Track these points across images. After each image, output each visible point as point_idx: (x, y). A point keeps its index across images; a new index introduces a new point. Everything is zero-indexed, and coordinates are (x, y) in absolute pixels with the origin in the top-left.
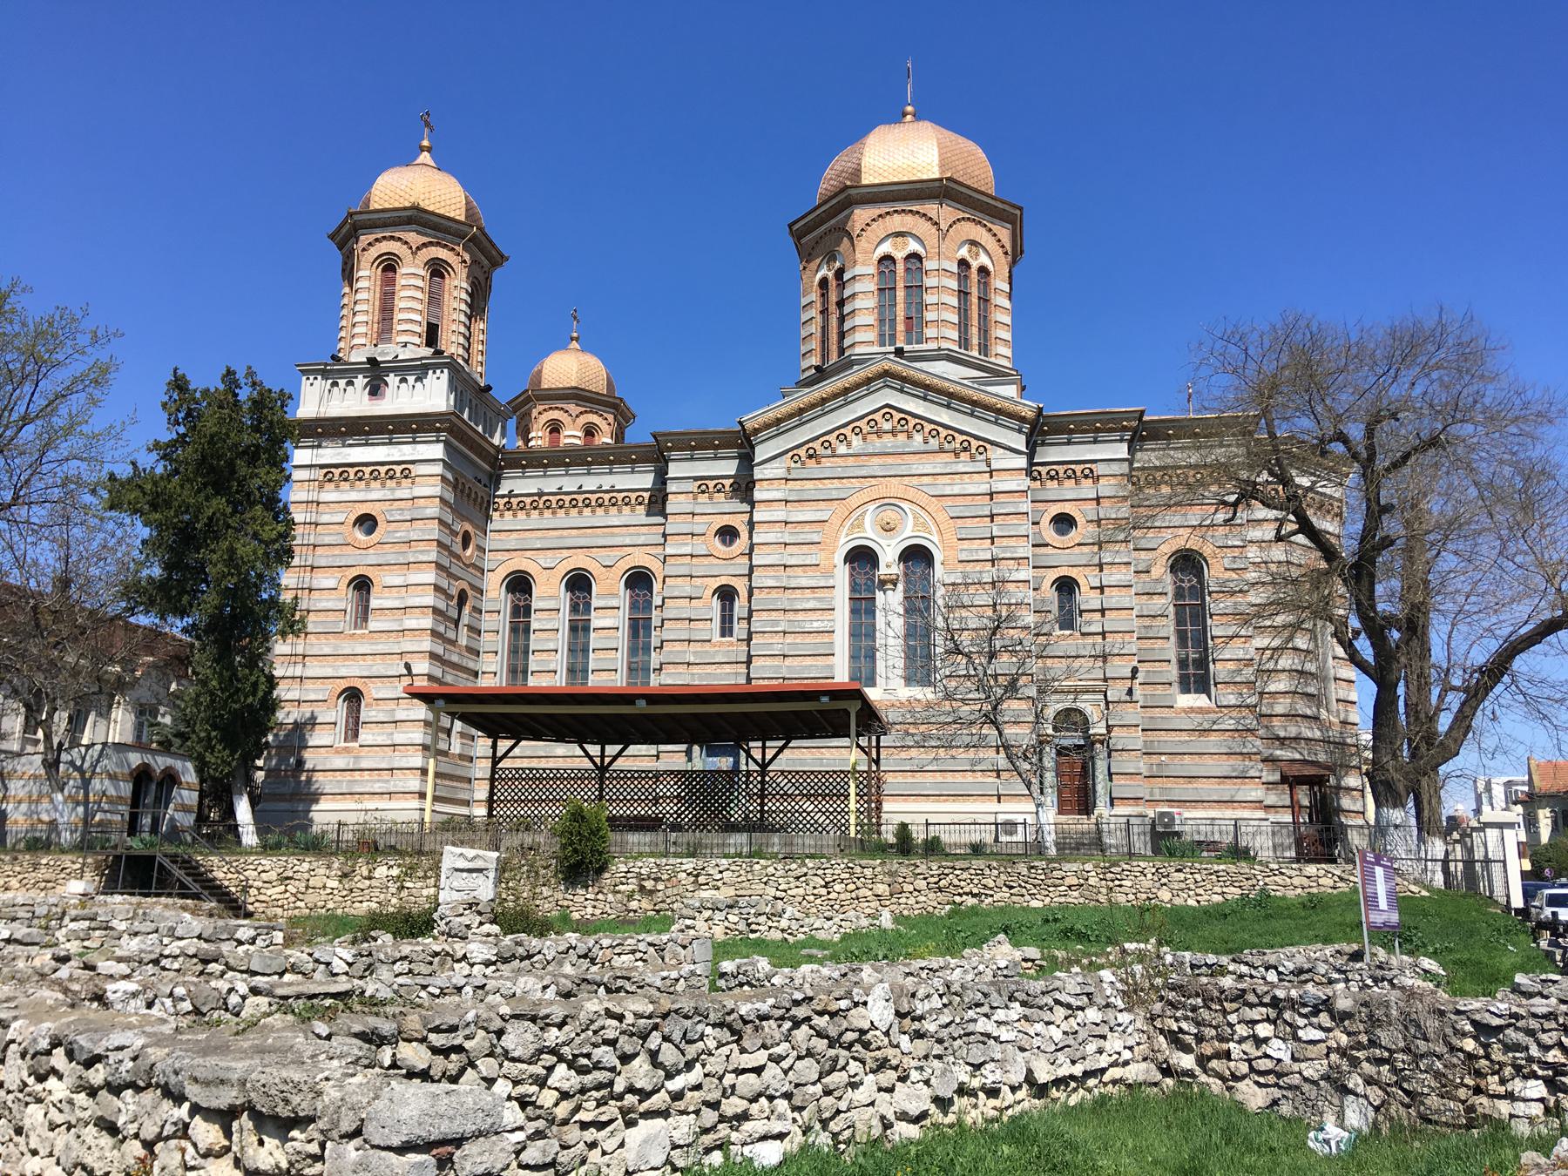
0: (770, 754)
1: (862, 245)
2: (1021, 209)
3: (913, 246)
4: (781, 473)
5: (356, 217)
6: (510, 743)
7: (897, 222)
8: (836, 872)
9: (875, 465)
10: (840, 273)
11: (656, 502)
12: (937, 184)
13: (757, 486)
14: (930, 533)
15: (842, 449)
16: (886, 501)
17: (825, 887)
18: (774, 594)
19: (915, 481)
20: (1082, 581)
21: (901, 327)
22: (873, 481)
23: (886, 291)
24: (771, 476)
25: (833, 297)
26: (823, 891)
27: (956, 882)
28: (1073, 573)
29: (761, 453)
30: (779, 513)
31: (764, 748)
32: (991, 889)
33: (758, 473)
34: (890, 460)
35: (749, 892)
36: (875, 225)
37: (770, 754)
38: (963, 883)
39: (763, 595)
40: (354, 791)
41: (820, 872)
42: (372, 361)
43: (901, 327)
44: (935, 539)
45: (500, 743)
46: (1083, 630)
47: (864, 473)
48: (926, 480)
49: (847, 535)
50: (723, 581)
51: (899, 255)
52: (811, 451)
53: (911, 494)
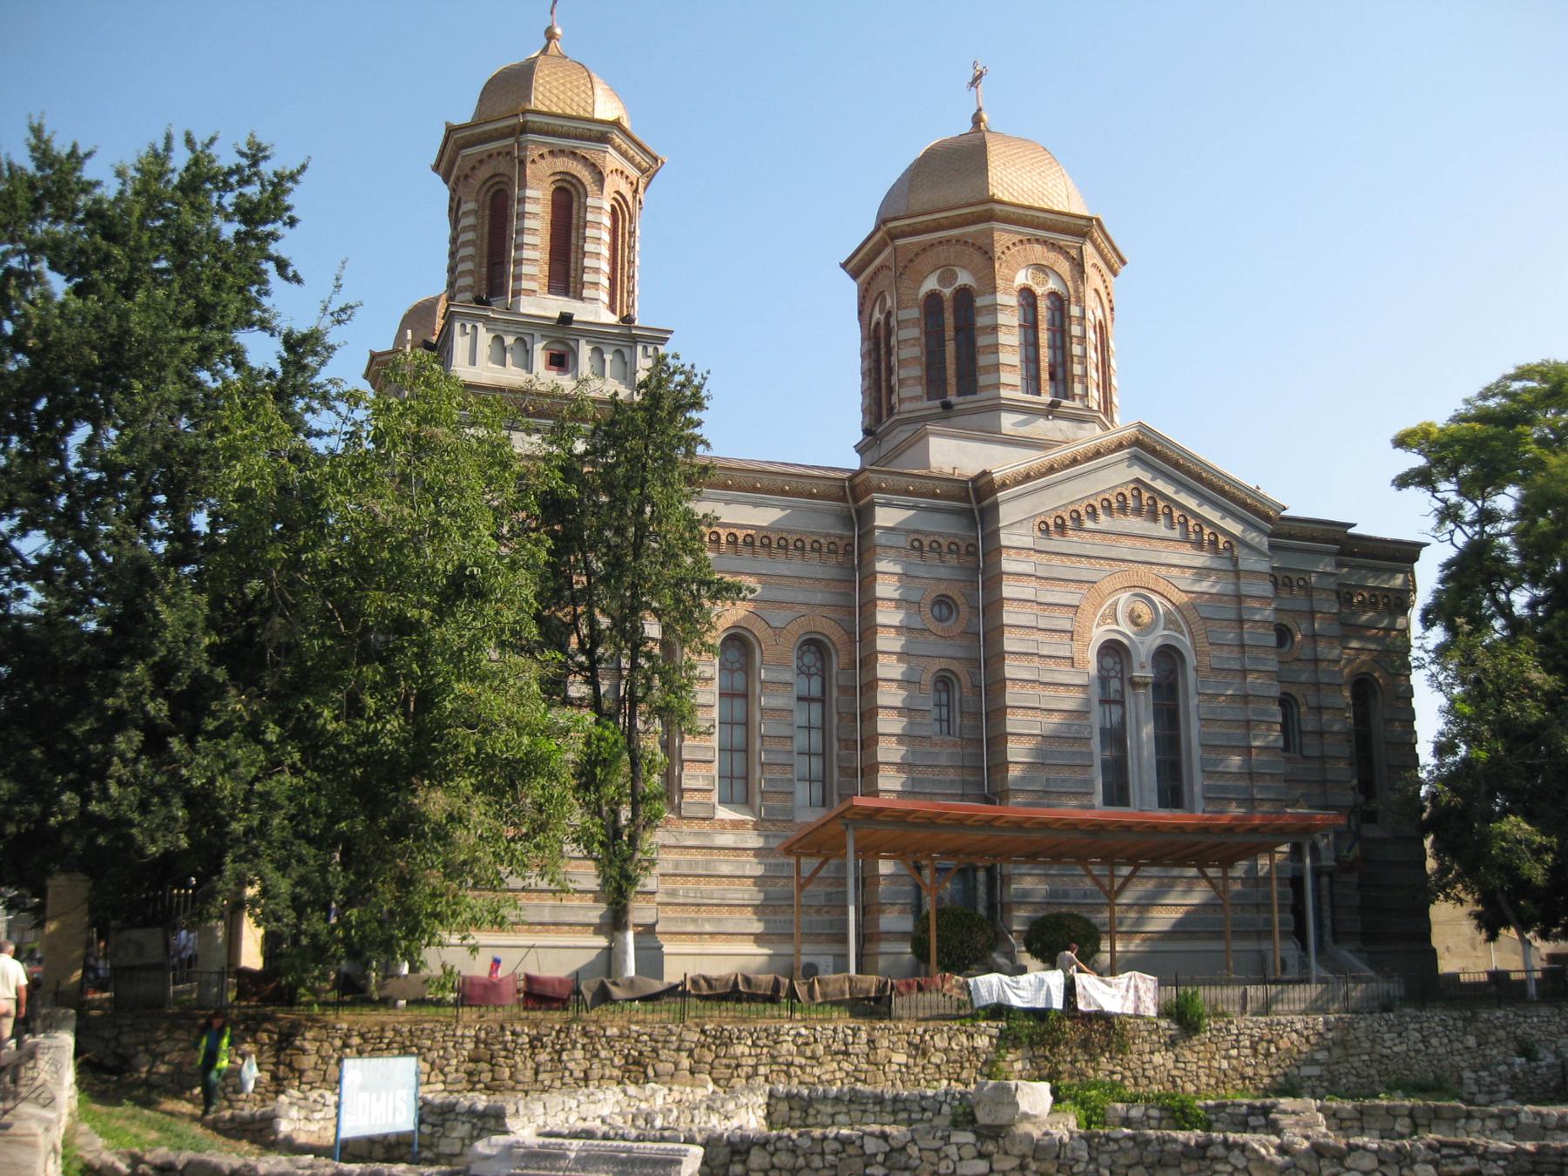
0: (1118, 882)
1: (1001, 270)
2: (1123, 262)
3: (1052, 284)
4: (1028, 542)
5: (530, 118)
6: (816, 862)
7: (1039, 253)
8: (1433, 1025)
9: (1124, 549)
10: (965, 297)
11: (835, 552)
12: (1083, 222)
13: (1004, 555)
14: (1182, 633)
15: (1089, 524)
16: (1138, 590)
17: (1423, 1042)
18: (1028, 690)
19: (1163, 571)
20: (1301, 700)
21: (1045, 376)
22: (1123, 566)
23: (1030, 326)
24: (1018, 544)
25: (949, 319)
26: (1421, 1046)
27: (1529, 1030)
28: (1293, 690)
29: (1009, 513)
30: (1026, 590)
31: (1112, 876)
32: (1555, 1035)
33: (1005, 539)
34: (1138, 543)
35: (1359, 1050)
36: (1014, 250)
37: (1118, 882)
38: (1534, 1032)
39: (1016, 689)
40: (561, 919)
41: (1417, 1026)
42: (566, 319)
43: (1045, 376)
44: (1187, 641)
45: (803, 860)
46: (1306, 753)
47: (1113, 554)
48: (1175, 572)
49: (1099, 625)
50: (943, 664)
51: (1039, 291)
52: (1059, 521)
53: (1162, 586)
